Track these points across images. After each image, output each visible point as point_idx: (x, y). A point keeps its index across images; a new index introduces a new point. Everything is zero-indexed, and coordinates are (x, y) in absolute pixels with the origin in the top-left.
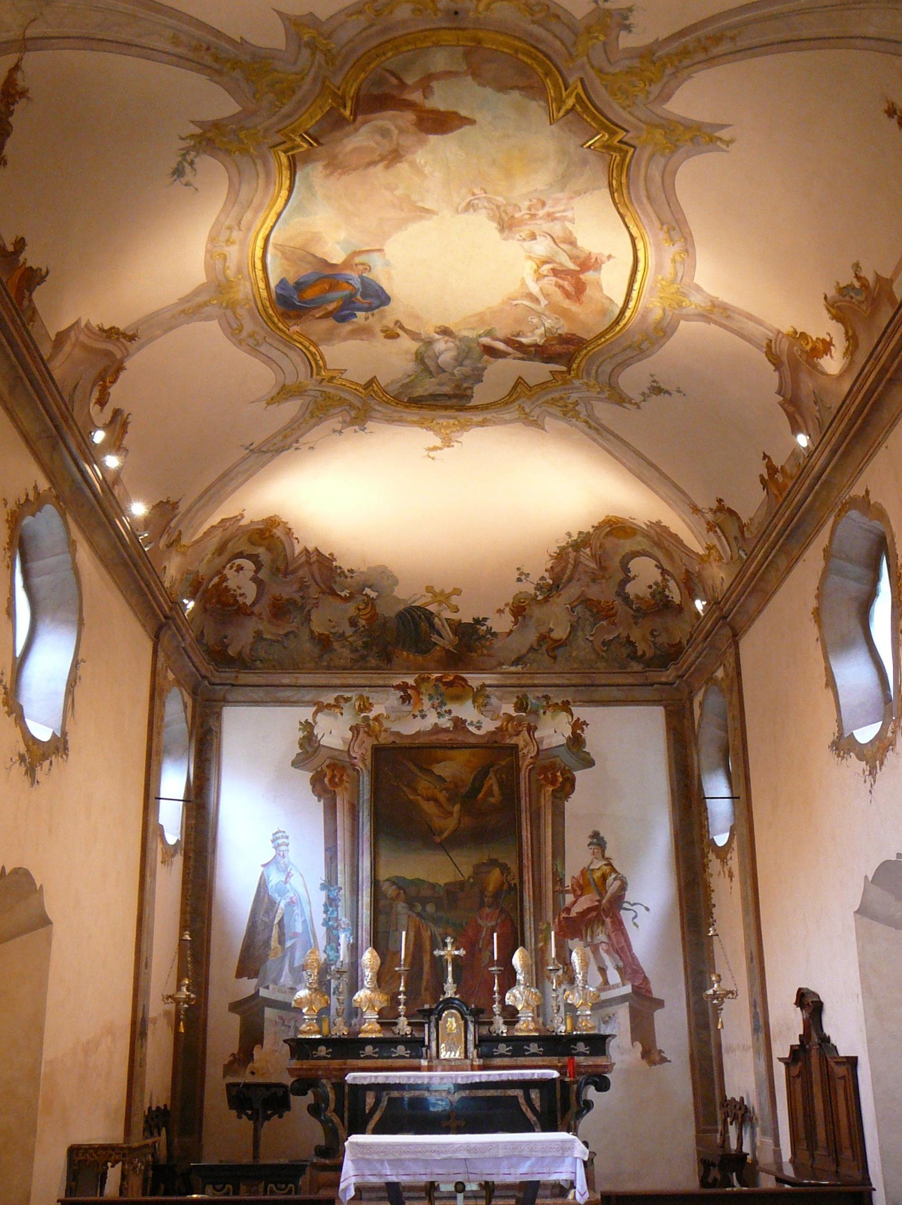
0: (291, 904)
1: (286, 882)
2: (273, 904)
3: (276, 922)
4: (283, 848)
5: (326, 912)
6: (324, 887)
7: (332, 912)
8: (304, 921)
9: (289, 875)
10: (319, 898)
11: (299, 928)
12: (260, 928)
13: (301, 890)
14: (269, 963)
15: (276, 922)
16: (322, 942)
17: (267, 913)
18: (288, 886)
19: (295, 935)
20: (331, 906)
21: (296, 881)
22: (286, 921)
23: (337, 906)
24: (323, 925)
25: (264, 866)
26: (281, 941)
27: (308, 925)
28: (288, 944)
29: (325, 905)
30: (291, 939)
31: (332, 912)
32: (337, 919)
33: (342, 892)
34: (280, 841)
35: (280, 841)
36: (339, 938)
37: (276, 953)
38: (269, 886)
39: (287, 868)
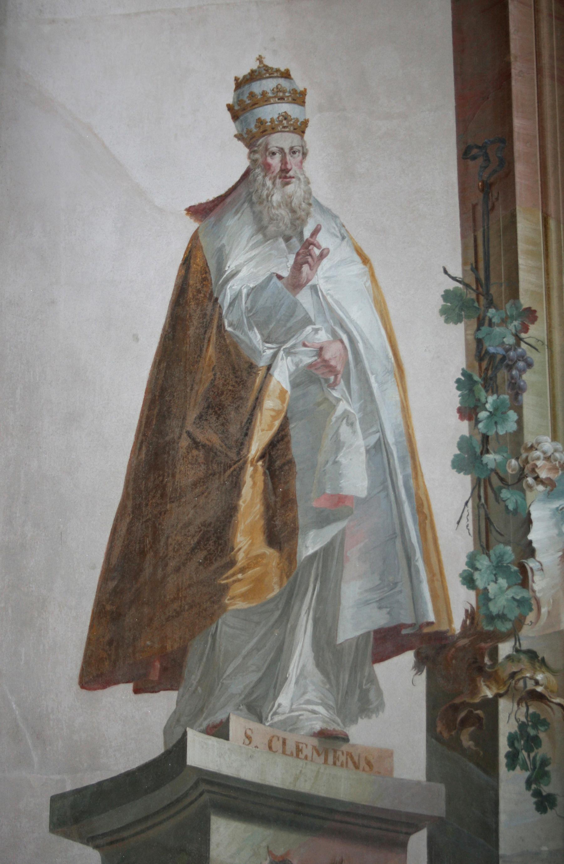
0: (319, 374)
1: (296, 283)
2: (240, 378)
3: (256, 446)
4: (282, 140)
5: (469, 411)
6: (456, 307)
7: (497, 415)
8: (378, 450)
9: (307, 255)
10: (438, 354)
11: (355, 478)
12: (187, 473)
13: (361, 317)
14: (226, 626)
15: (256, 446)
16: (456, 541)
17: (215, 408)
18: (305, 298)
19: (339, 506)
20: (490, 385)
21: (338, 279)
22: (298, 448)
23: (517, 390)
24: (459, 465)
25: (199, 212)
26: (280, 532)
27: (395, 462)
28: (310, 544)
29: (466, 384)
30: (323, 520)
31: (497, 415)
32: (516, 443)
33: (536, 331)
34: (270, 112)
35: (270, 112)
36: (527, 523)
37: (259, 584)
38: (226, 300)
39: (298, 222)
